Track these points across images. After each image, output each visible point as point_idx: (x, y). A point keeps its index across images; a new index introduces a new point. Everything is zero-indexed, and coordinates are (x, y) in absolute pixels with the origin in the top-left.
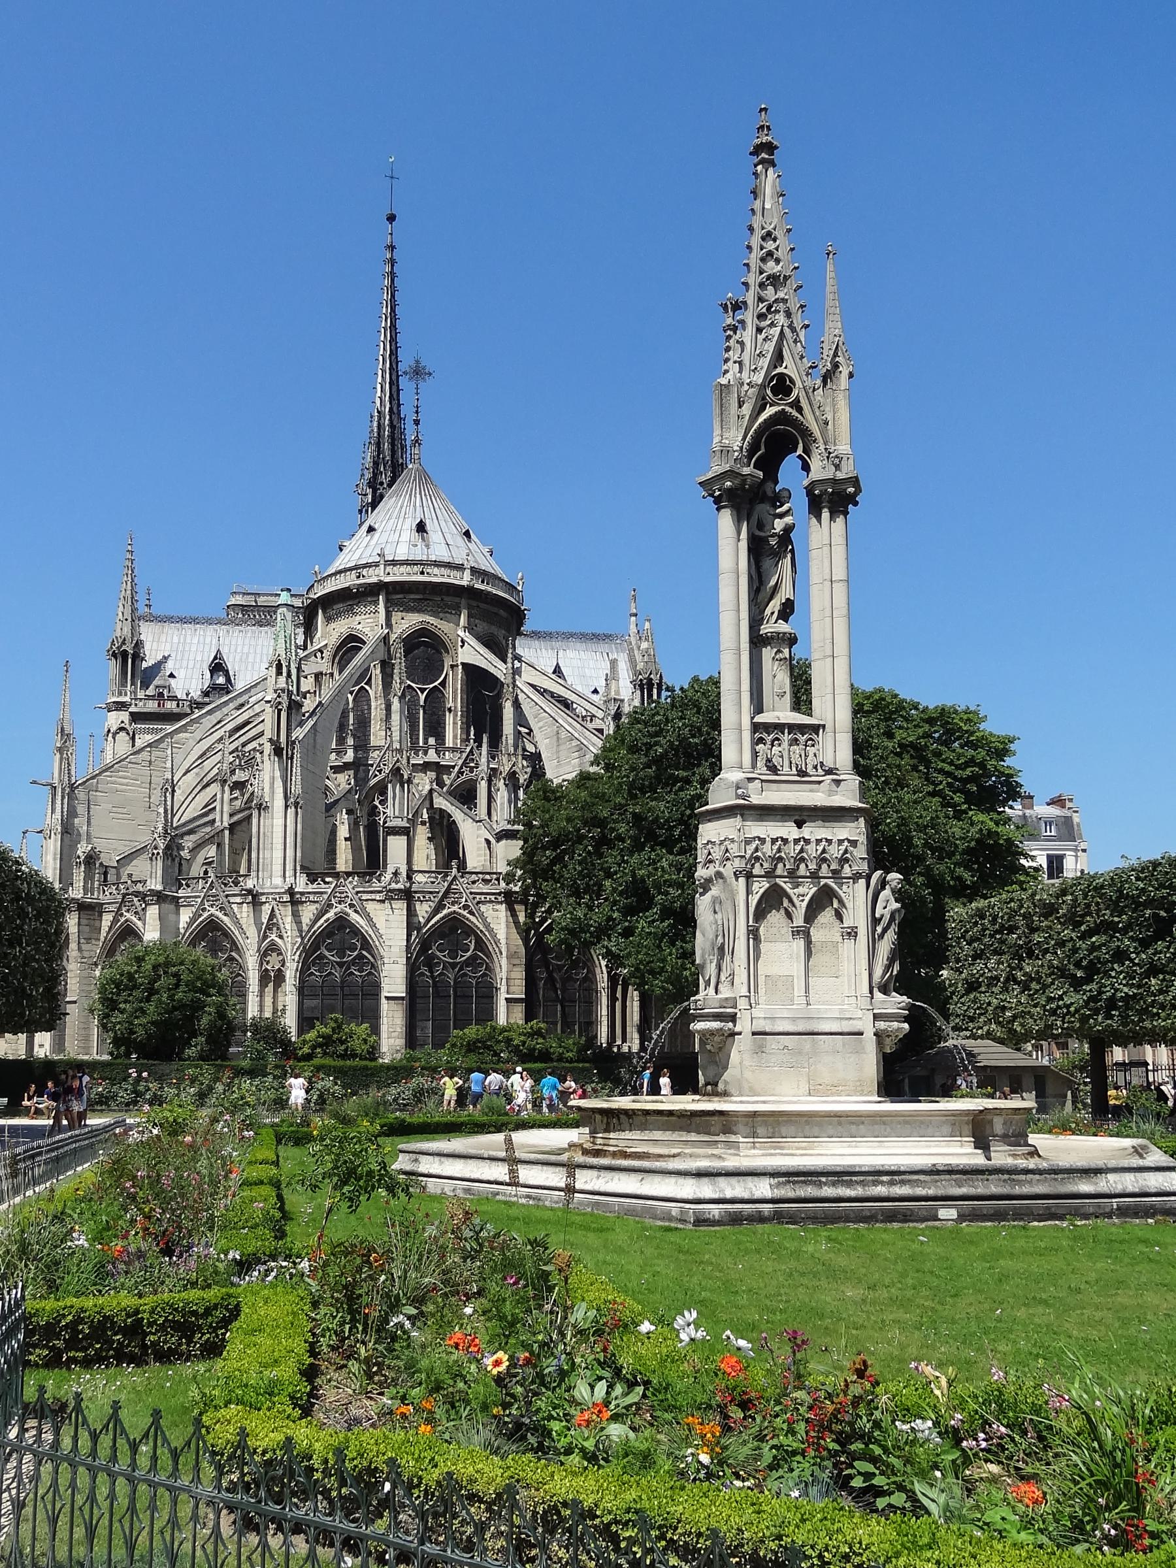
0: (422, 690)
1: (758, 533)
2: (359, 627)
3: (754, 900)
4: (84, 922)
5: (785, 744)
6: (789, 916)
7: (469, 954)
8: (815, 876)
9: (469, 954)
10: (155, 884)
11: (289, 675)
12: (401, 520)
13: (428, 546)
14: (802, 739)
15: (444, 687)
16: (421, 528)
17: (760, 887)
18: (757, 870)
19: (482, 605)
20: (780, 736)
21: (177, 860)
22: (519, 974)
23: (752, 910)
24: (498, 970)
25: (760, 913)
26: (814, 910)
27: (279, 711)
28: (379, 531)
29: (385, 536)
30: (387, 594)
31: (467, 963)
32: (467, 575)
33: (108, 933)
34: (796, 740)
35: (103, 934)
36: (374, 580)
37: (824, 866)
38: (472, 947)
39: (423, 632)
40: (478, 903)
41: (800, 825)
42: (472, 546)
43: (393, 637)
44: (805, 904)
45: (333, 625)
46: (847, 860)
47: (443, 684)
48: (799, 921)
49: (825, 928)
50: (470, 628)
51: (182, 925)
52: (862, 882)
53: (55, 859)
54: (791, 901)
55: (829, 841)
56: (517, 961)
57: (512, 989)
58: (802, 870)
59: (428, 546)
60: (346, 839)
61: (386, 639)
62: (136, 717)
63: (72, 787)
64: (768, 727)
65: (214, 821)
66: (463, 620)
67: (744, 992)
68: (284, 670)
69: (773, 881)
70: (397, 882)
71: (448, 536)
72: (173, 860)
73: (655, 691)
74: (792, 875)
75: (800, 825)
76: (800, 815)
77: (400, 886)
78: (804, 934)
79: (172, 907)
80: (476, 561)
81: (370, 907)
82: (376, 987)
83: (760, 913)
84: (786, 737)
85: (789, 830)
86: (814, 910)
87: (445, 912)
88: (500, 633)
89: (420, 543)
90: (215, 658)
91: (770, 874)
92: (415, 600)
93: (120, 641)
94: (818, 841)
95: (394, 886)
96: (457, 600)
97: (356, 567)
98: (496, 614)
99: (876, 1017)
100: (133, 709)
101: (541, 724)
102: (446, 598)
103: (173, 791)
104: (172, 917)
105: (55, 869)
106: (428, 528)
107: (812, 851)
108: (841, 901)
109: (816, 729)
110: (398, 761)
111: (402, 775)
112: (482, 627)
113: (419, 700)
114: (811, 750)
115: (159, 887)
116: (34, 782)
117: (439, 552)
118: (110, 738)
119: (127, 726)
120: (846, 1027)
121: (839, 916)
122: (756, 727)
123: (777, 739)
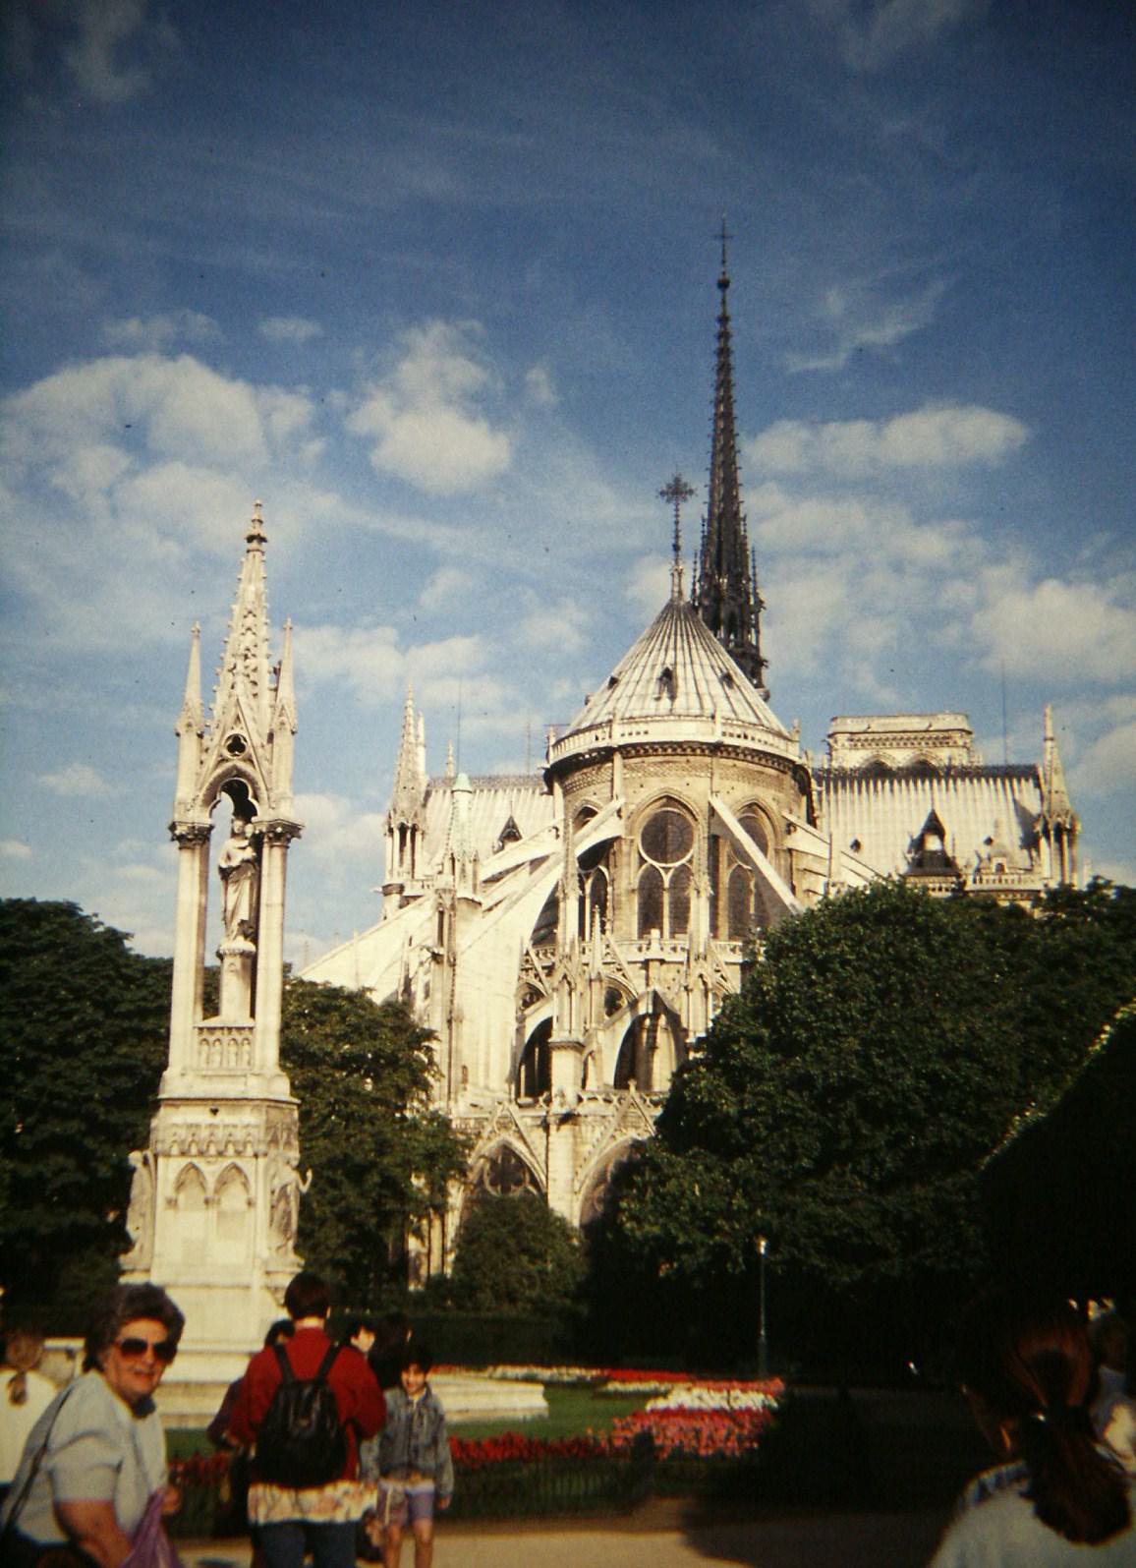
0: (667, 870)
1: (224, 866)
2: (594, 799)
3: (172, 1176)
6: (202, 1185)
8: (220, 1154)
11: (463, 871)
13: (673, 698)
14: (239, 1038)
16: (668, 677)
19: (739, 763)
26: (223, 1183)
27: (442, 914)
30: (624, 758)
32: (719, 728)
34: (234, 1040)
41: (215, 1112)
42: (733, 694)
46: (249, 1142)
47: (690, 861)
48: (210, 1193)
49: (234, 1198)
55: (235, 1126)
59: (673, 698)
64: (212, 1030)
68: (458, 865)
69: (189, 1160)
74: (201, 1153)
75: (215, 1112)
76: (214, 1105)
80: (734, 712)
83: (180, 1185)
84: (226, 1038)
86: (223, 1183)
88: (767, 796)
89: (665, 695)
90: (507, 826)
92: (655, 764)
94: (226, 1126)
97: (590, 728)
98: (762, 773)
102: (691, 758)
106: (680, 671)
107: (220, 1134)
108: (246, 1177)
113: (662, 881)
114: (246, 1047)
121: (245, 1184)
123: (219, 1040)
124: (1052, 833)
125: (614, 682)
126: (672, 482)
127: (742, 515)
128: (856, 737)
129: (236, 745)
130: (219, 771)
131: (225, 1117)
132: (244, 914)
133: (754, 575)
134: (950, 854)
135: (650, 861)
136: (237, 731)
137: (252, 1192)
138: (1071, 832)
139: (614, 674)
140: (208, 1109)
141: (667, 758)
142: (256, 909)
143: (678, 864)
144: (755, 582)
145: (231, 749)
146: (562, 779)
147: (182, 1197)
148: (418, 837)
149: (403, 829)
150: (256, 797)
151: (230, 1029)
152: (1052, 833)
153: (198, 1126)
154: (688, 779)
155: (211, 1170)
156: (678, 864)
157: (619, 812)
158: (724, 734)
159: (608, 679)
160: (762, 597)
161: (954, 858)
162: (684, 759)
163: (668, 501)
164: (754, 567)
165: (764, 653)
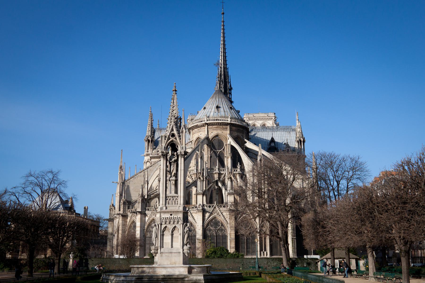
3: (162, 229)
4: (123, 220)
5: (172, 200)
6: (169, 232)
7: (220, 227)
9: (220, 227)
10: (139, 210)
12: (212, 105)
13: (219, 112)
15: (224, 151)
17: (163, 226)
18: (163, 223)
20: (171, 198)
21: (145, 203)
22: (233, 233)
23: (162, 230)
24: (227, 231)
25: (163, 232)
28: (206, 109)
29: (208, 110)
31: (219, 229)
32: (229, 120)
33: (129, 222)
35: (128, 223)
36: (204, 122)
37: (175, 223)
38: (221, 225)
39: (217, 136)
40: (222, 213)
41: (171, 215)
43: (210, 137)
44: (171, 229)
45: (194, 135)
49: (176, 233)
50: (231, 134)
51: (146, 220)
52: (182, 225)
53: (118, 203)
54: (169, 229)
56: (232, 229)
57: (231, 236)
58: (172, 223)
59: (219, 112)
60: (194, 194)
61: (207, 138)
62: (151, 158)
63: (123, 183)
65: (157, 192)
66: (228, 132)
67: (159, 245)
70: (200, 208)
71: (225, 109)
72: (144, 203)
73: (302, 143)
75: (171, 215)
77: (200, 209)
78: (172, 235)
79: (144, 216)
81: (193, 214)
82: (195, 236)
85: (168, 216)
87: (213, 215)
88: (240, 135)
91: (166, 223)
92: (215, 127)
93: (148, 136)
95: (199, 209)
96: (227, 127)
99: (183, 250)
100: (151, 156)
101: (245, 162)
102: (224, 126)
103: (148, 183)
104: (144, 218)
105: (118, 205)
109: (177, 197)
110: (199, 175)
111: (201, 179)
112: (236, 134)
114: (177, 200)
115: (140, 210)
116: (113, 182)
117: (223, 114)
118: (145, 163)
119: (150, 161)
120: (178, 251)
122: (166, 197)
124: (299, 142)
125: (205, 108)
126: (217, 62)
127: (227, 68)
128: (250, 118)
129: (173, 135)
130: (170, 141)
131: (174, 216)
132: (174, 172)
133: (230, 82)
134: (276, 147)
135: (214, 150)
136: (173, 132)
137: (180, 232)
138: (304, 142)
139: (205, 106)
140: (169, 214)
141: (218, 126)
142: (177, 170)
143: (220, 151)
144: (230, 83)
145: (172, 136)
146: (192, 130)
147: (164, 233)
148: (153, 142)
149: (149, 141)
150: (177, 147)
151: (173, 197)
152: (299, 142)
153: (167, 218)
154: (223, 131)
155: (170, 227)
156: (220, 151)
157: (207, 138)
158: (231, 121)
159: (203, 108)
160: (232, 87)
161: (277, 148)
162: (221, 126)
163: (216, 66)
164: (230, 80)
165: (233, 100)
